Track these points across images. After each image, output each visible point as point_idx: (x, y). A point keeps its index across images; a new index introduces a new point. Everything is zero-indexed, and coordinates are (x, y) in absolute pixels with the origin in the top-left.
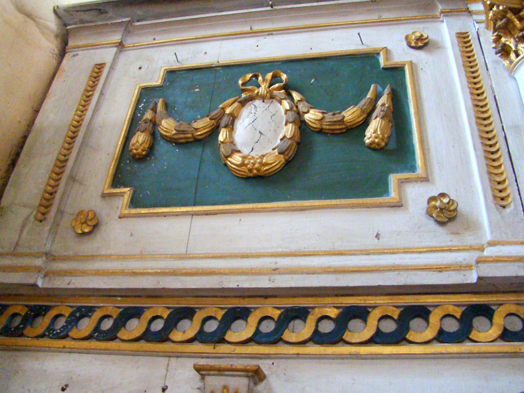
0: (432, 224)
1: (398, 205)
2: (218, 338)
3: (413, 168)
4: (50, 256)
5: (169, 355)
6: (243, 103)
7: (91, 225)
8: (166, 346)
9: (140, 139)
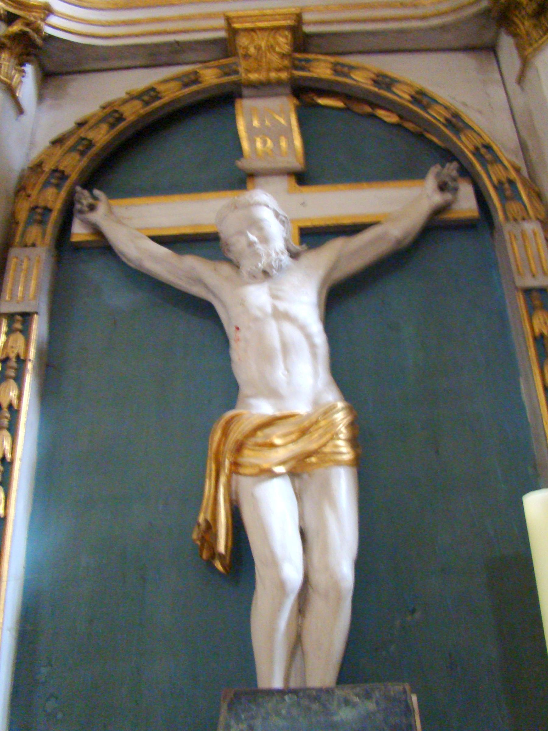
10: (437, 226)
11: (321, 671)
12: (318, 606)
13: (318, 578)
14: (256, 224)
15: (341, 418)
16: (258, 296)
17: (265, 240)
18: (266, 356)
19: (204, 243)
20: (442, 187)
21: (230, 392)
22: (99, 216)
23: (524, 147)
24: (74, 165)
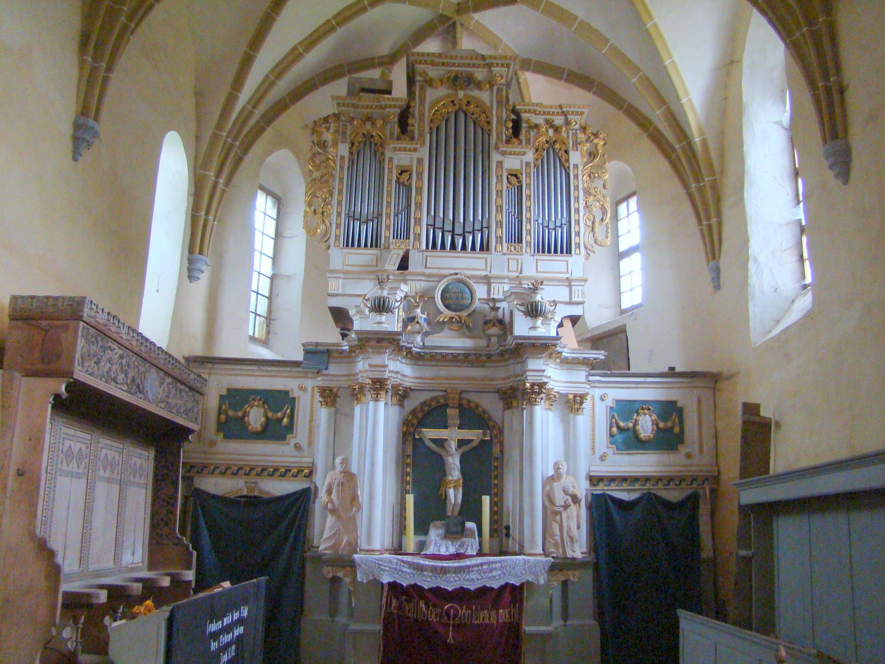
1: (288, 444)
4: (204, 453)
7: (213, 443)
9: (223, 417)
10: (482, 441)
11: (456, 513)
16: (450, 459)
19: (441, 443)
24: (415, 422)
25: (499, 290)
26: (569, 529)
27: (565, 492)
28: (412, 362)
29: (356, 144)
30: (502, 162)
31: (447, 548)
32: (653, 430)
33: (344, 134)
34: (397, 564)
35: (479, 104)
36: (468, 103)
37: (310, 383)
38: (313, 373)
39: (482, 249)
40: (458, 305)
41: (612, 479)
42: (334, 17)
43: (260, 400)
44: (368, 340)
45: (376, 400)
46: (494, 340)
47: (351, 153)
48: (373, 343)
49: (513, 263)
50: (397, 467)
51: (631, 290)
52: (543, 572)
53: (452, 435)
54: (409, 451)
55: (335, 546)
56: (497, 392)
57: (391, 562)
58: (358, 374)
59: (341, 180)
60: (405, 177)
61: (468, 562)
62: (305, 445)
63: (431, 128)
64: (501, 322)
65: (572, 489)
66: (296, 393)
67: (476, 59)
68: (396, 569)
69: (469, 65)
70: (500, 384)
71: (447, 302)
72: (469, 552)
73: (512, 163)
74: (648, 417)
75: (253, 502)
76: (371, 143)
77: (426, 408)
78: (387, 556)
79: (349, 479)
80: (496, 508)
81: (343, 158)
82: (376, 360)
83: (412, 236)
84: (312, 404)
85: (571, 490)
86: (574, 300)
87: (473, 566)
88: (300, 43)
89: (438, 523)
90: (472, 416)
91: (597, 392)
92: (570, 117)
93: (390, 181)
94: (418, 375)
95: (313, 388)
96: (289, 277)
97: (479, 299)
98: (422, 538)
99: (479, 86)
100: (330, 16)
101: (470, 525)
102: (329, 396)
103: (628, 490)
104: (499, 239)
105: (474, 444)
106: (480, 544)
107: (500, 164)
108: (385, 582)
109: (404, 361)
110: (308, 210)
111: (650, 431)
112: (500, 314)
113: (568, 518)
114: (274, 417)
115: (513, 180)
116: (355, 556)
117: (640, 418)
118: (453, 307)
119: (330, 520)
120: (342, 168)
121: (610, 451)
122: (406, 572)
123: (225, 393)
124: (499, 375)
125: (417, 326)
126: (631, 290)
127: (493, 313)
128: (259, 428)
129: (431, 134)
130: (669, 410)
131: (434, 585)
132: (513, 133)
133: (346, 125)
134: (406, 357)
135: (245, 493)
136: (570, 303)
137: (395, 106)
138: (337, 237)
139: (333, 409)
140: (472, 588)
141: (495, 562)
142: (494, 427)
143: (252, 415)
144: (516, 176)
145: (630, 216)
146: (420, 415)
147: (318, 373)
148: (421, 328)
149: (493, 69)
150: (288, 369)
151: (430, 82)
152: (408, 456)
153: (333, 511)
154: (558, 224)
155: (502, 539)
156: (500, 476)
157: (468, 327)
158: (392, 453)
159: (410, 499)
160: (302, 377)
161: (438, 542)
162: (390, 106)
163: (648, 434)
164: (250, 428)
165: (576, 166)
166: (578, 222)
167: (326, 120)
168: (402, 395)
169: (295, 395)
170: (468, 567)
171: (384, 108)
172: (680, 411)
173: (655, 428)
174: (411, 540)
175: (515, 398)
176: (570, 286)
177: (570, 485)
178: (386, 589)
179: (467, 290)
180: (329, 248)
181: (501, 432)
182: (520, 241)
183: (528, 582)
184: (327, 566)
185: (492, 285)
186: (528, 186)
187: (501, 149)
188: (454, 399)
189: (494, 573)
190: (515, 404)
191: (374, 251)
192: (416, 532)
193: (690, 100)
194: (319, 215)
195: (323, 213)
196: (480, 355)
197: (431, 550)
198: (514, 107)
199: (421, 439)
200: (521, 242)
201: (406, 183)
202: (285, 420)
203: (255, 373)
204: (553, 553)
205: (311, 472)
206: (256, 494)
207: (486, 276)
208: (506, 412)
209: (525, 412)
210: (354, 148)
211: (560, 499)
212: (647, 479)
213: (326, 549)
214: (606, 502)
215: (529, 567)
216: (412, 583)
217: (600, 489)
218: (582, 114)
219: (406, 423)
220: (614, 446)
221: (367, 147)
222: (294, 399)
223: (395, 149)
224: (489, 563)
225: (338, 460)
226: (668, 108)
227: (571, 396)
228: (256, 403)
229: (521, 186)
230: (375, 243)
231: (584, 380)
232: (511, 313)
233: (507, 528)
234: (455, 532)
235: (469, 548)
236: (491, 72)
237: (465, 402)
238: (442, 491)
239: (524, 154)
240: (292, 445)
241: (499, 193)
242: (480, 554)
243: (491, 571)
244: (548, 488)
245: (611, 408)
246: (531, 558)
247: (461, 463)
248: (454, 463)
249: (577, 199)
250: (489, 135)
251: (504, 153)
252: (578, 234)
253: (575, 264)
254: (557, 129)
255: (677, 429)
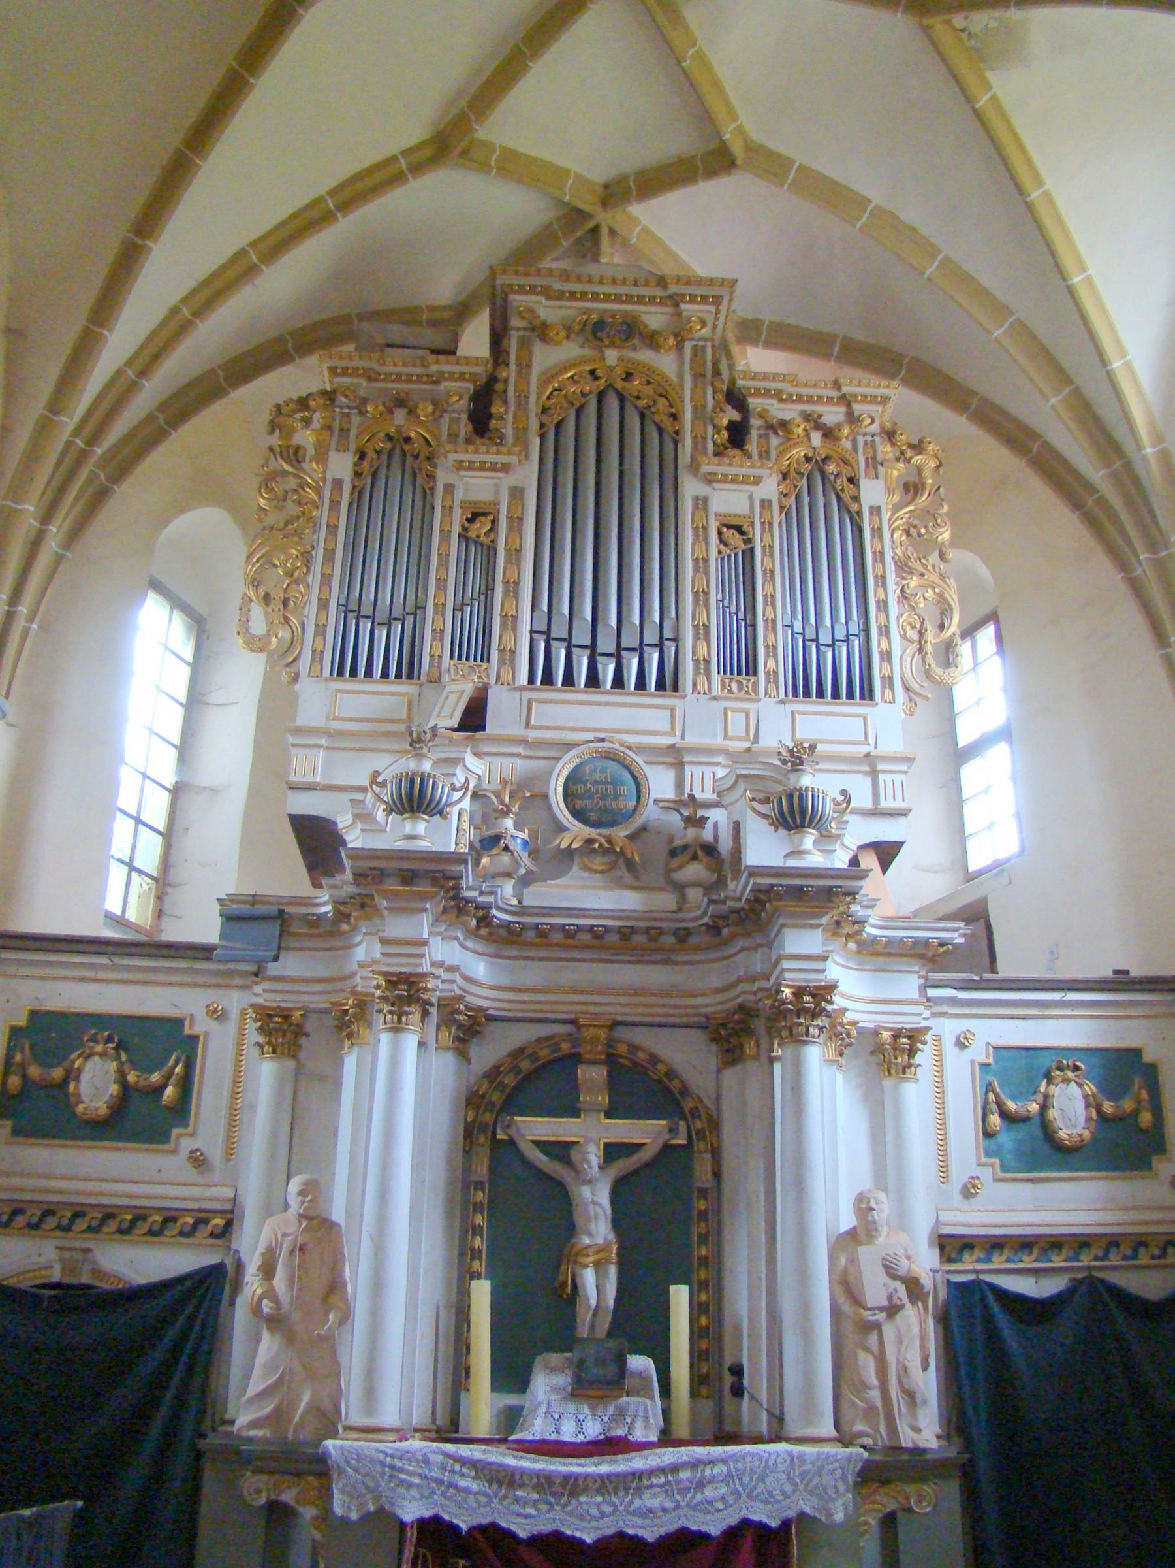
0: (189, 1167)
1: (175, 1152)
2: (68, 1229)
3: (187, 1126)
5: (41, 1237)
6: (87, 1058)
8: (39, 1232)
10: (667, 1148)
11: (601, 1332)
12: (601, 1313)
13: (602, 1304)
14: (589, 1162)
15: (615, 1247)
16: (586, 1192)
17: (590, 1167)
18: (588, 1219)
19: (561, 1150)
20: (671, 1131)
21: (570, 1228)
22: (512, 1131)
23: (718, 1097)
24: (497, 1097)
25: (703, 781)
26: (904, 1369)
27: (890, 1270)
28: (492, 949)
29: (371, 455)
30: (705, 500)
31: (580, 1423)
32: (1088, 1119)
33: (345, 432)
34: (443, 1468)
35: (652, 378)
36: (628, 376)
37: (235, 1001)
38: (245, 974)
39: (661, 686)
40: (605, 810)
41: (995, 1244)
42: (332, 193)
43: (109, 1039)
44: (381, 875)
45: (397, 1028)
46: (694, 894)
47: (358, 474)
48: (392, 885)
49: (737, 723)
50: (449, 1214)
51: (990, 827)
52: (841, 1487)
53: (591, 1132)
54: (481, 1170)
55: (278, 1417)
56: (704, 1027)
57: (426, 1461)
58: (354, 974)
59: (332, 529)
60: (480, 528)
61: (637, 1462)
62: (215, 1154)
63: (542, 426)
64: (710, 850)
65: (905, 1263)
66: (201, 1025)
67: (646, 284)
68: (440, 1482)
69: (629, 299)
70: (713, 1005)
71: (579, 804)
72: (639, 1435)
73: (729, 501)
74: (1073, 1089)
75: (73, 1300)
76: (404, 455)
77: (525, 1065)
78: (416, 1444)
79: (320, 1236)
80: (703, 1321)
81: (338, 484)
82: (399, 927)
83: (495, 655)
84: (239, 1052)
85: (904, 1266)
86: (883, 804)
87: (651, 1473)
88: (253, 244)
89: (556, 1358)
90: (641, 1086)
91: (948, 1028)
92: (857, 408)
93: (446, 535)
94: (504, 981)
95: (243, 1013)
96: (214, 791)
97: (656, 801)
98: (511, 1399)
99: (652, 340)
100: (322, 191)
101: (639, 1363)
102: (283, 1031)
103: (1035, 1272)
104: (702, 665)
105: (645, 1155)
106: (666, 1413)
107: (701, 503)
108: (408, 1517)
109: (469, 944)
110: (251, 594)
111: (1082, 1120)
112: (707, 835)
113: (900, 1340)
114: (142, 1083)
115: (735, 538)
116: (329, 1443)
117: (1053, 1089)
118: (593, 816)
119: (268, 1344)
120: (335, 505)
121: (986, 1174)
122: (467, 1490)
123: (22, 1022)
124: (706, 982)
125: (506, 858)
126: (990, 827)
127: (692, 832)
128: (103, 1110)
129: (543, 437)
130: (1124, 1070)
131: (546, 1528)
132: (729, 441)
133: (348, 415)
134: (474, 934)
135: (56, 1275)
136: (876, 812)
137: (462, 377)
138: (317, 656)
139: (290, 1063)
140: (650, 1534)
141: (712, 1462)
142: (695, 1113)
143: (85, 1077)
144: (739, 529)
145: (980, 669)
146: (510, 1081)
147: (256, 975)
148: (518, 865)
149: (683, 306)
150: (183, 964)
151: (541, 331)
152: (479, 1185)
153: (275, 1322)
154: (840, 634)
155: (723, 1399)
156: (714, 1236)
157: (630, 865)
158: (437, 1175)
159: (481, 1293)
160: (218, 986)
161: (553, 1407)
162: (451, 377)
163: (1079, 1130)
164: (80, 1108)
165: (876, 511)
166: (885, 631)
167: (303, 403)
168: (465, 1027)
169: (198, 1029)
170: (638, 1475)
171: (437, 382)
172: (1151, 1073)
173: (1094, 1115)
174: (483, 1405)
175: (750, 1033)
176: (874, 774)
177: (901, 1252)
178: (412, 1535)
179: (628, 776)
180: (296, 678)
181: (715, 1124)
182: (751, 670)
183: (802, 1515)
184: (258, 1471)
185: (688, 768)
186: (769, 550)
187: (705, 469)
188: (595, 1040)
189: (709, 1492)
190: (749, 1048)
191: (405, 688)
192: (497, 1385)
193: (1128, 365)
194: (276, 605)
195: (285, 602)
196: (661, 931)
197: (537, 1428)
198: (733, 382)
199: (512, 1142)
200: (755, 673)
201: (483, 539)
202: (170, 1090)
203: (101, 975)
204: (862, 1434)
205: (229, 1224)
206: (85, 1279)
207: (673, 746)
208: (728, 1073)
209: (777, 1067)
210: (365, 465)
211: (876, 1288)
212: (1082, 1243)
213: (255, 1424)
214: (984, 1299)
215: (802, 1475)
216: (485, 1521)
217: (967, 1268)
218: (885, 400)
219: (473, 1100)
220: (996, 1161)
221: (397, 465)
222: (194, 1038)
223: (459, 465)
224: (695, 1464)
225: (294, 1186)
226: (1077, 392)
227: (886, 1035)
228: (99, 1048)
229: (752, 550)
230: (408, 669)
231: (915, 995)
232: (737, 827)
233: (737, 1371)
234: (599, 1382)
235: (639, 1424)
236: (679, 314)
237: (622, 1049)
238: (566, 1271)
239: (757, 481)
240: (184, 1154)
241: (701, 564)
242: (667, 1439)
243: (701, 1485)
244: (843, 1260)
245: (984, 1066)
246: (809, 1450)
247: (613, 1202)
248: (595, 1199)
249: (882, 580)
250: (676, 443)
251: (710, 479)
252: (887, 656)
253: (886, 723)
254: (829, 434)
255: (1146, 1118)
